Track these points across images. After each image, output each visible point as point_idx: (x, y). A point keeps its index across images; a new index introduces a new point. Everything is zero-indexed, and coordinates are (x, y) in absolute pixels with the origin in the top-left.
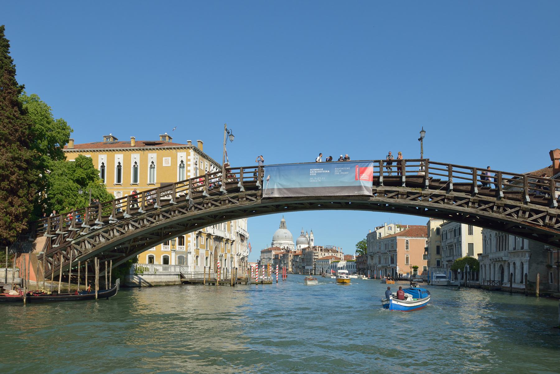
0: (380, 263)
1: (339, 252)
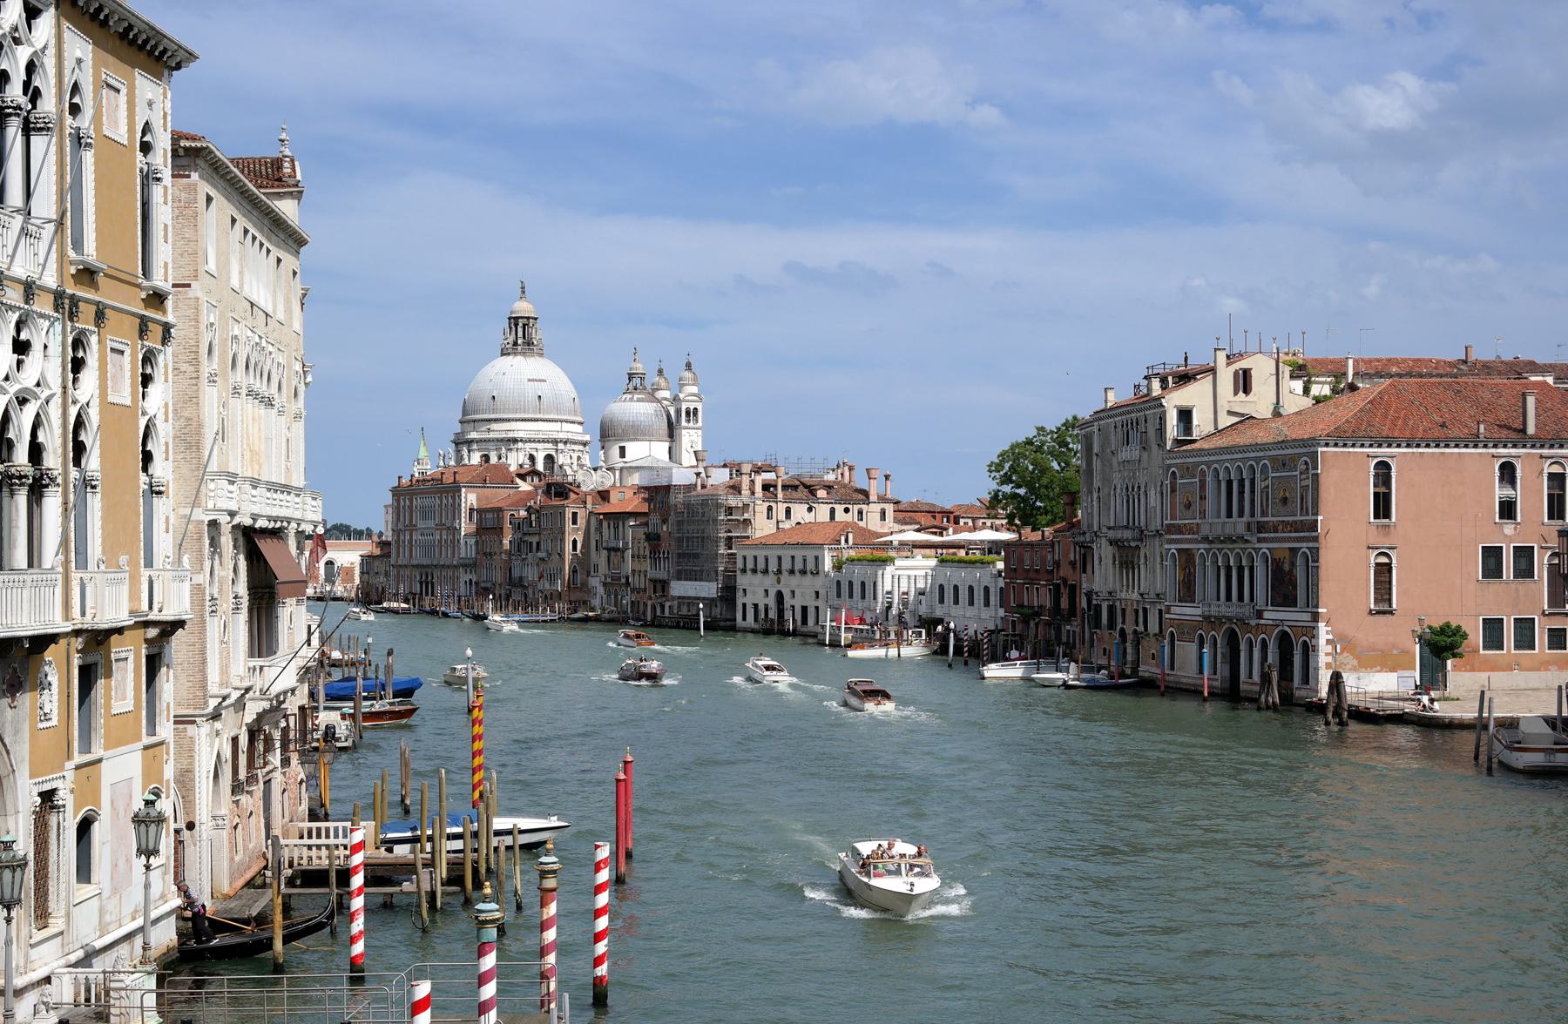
0: (1187, 592)
1: (873, 498)
